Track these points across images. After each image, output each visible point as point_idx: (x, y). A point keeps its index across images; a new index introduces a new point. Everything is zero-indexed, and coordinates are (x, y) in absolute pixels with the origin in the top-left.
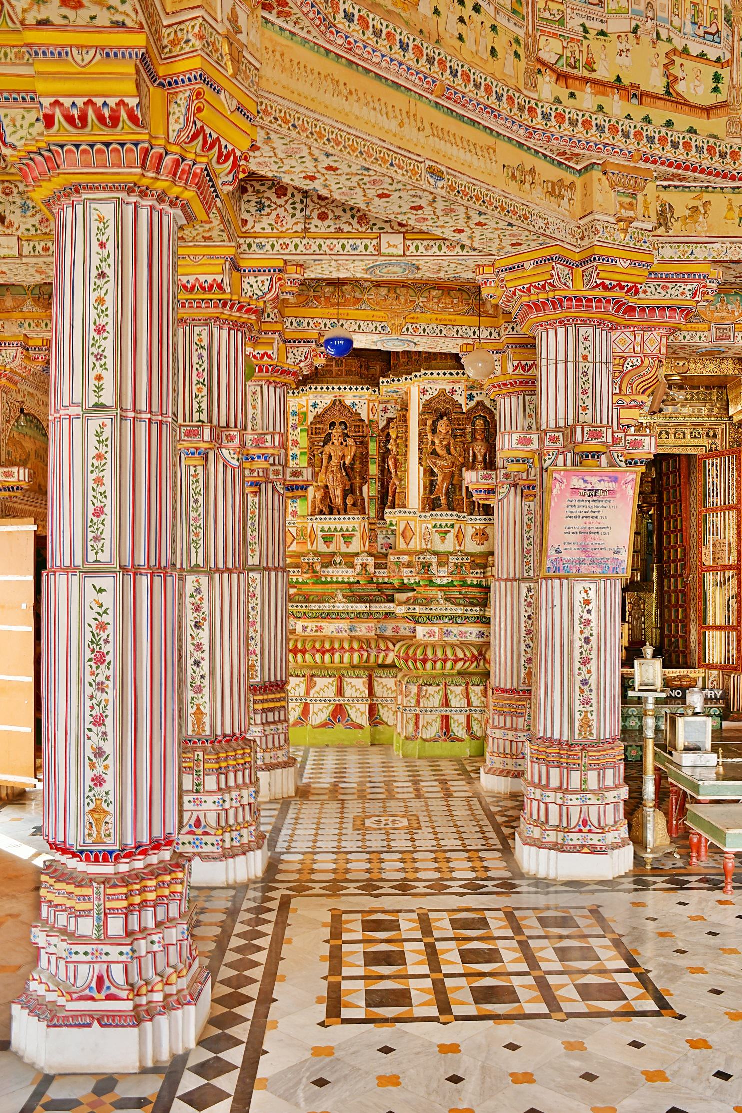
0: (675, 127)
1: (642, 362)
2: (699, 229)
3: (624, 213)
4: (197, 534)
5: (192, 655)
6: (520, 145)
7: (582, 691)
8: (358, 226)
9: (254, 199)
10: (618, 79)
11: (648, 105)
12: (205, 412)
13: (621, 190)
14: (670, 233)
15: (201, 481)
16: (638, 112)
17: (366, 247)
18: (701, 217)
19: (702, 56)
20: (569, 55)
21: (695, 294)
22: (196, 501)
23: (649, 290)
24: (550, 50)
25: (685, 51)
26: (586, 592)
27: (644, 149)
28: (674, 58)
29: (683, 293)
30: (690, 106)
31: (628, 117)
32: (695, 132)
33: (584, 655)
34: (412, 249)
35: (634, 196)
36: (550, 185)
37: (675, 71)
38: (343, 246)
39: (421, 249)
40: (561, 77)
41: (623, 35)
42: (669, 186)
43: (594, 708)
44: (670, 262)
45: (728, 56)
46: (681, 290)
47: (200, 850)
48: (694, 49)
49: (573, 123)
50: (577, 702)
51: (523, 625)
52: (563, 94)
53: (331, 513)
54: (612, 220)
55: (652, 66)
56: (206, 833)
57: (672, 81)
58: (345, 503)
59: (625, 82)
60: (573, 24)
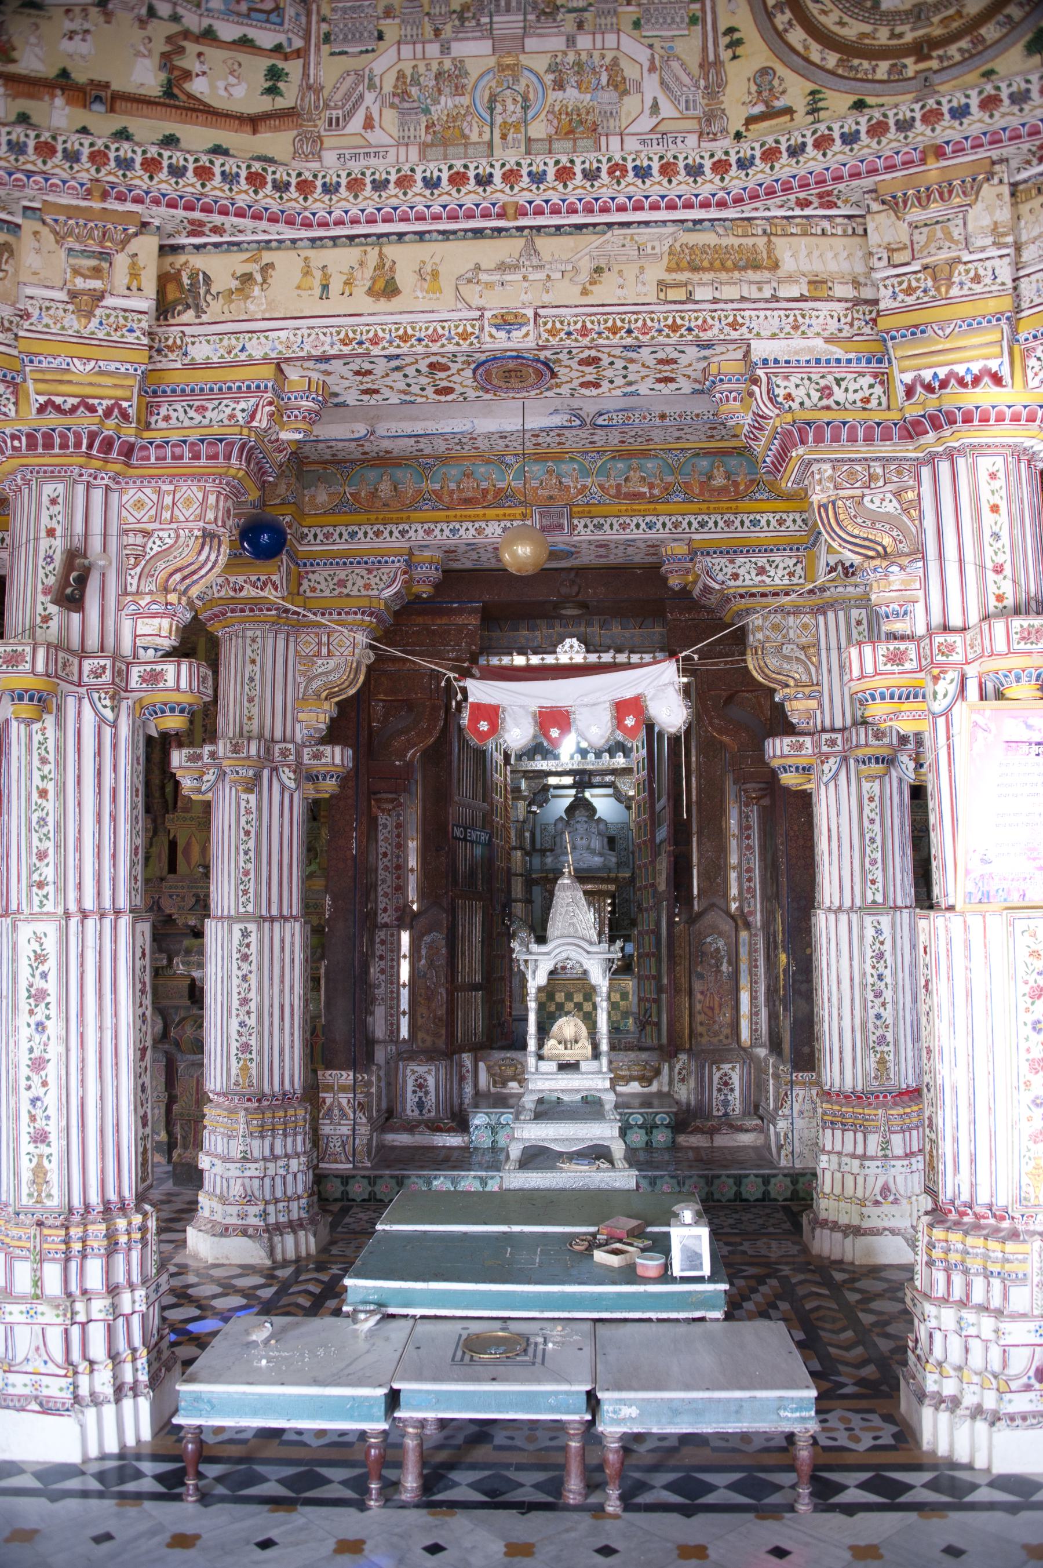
0: (183, 145)
1: (178, 536)
2: (252, 308)
3: (80, 283)
7: (33, 1118)
11: (125, 112)
13: (77, 246)
14: (205, 318)
16: (103, 123)
18: (257, 291)
19: (244, 43)
21: (253, 417)
23: (174, 415)
25: (208, 36)
26: (38, 939)
27: (111, 178)
28: (185, 43)
29: (232, 417)
30: (208, 112)
31: (84, 131)
32: (225, 153)
33: (36, 1054)
35: (105, 256)
42: (205, 245)
43: (54, 1149)
44: (207, 366)
45: (298, 43)
46: (228, 411)
50: (25, 1138)
51: (235, 990)
54: (63, 296)
55: (138, 54)
57: (175, 80)
59: (80, 77)
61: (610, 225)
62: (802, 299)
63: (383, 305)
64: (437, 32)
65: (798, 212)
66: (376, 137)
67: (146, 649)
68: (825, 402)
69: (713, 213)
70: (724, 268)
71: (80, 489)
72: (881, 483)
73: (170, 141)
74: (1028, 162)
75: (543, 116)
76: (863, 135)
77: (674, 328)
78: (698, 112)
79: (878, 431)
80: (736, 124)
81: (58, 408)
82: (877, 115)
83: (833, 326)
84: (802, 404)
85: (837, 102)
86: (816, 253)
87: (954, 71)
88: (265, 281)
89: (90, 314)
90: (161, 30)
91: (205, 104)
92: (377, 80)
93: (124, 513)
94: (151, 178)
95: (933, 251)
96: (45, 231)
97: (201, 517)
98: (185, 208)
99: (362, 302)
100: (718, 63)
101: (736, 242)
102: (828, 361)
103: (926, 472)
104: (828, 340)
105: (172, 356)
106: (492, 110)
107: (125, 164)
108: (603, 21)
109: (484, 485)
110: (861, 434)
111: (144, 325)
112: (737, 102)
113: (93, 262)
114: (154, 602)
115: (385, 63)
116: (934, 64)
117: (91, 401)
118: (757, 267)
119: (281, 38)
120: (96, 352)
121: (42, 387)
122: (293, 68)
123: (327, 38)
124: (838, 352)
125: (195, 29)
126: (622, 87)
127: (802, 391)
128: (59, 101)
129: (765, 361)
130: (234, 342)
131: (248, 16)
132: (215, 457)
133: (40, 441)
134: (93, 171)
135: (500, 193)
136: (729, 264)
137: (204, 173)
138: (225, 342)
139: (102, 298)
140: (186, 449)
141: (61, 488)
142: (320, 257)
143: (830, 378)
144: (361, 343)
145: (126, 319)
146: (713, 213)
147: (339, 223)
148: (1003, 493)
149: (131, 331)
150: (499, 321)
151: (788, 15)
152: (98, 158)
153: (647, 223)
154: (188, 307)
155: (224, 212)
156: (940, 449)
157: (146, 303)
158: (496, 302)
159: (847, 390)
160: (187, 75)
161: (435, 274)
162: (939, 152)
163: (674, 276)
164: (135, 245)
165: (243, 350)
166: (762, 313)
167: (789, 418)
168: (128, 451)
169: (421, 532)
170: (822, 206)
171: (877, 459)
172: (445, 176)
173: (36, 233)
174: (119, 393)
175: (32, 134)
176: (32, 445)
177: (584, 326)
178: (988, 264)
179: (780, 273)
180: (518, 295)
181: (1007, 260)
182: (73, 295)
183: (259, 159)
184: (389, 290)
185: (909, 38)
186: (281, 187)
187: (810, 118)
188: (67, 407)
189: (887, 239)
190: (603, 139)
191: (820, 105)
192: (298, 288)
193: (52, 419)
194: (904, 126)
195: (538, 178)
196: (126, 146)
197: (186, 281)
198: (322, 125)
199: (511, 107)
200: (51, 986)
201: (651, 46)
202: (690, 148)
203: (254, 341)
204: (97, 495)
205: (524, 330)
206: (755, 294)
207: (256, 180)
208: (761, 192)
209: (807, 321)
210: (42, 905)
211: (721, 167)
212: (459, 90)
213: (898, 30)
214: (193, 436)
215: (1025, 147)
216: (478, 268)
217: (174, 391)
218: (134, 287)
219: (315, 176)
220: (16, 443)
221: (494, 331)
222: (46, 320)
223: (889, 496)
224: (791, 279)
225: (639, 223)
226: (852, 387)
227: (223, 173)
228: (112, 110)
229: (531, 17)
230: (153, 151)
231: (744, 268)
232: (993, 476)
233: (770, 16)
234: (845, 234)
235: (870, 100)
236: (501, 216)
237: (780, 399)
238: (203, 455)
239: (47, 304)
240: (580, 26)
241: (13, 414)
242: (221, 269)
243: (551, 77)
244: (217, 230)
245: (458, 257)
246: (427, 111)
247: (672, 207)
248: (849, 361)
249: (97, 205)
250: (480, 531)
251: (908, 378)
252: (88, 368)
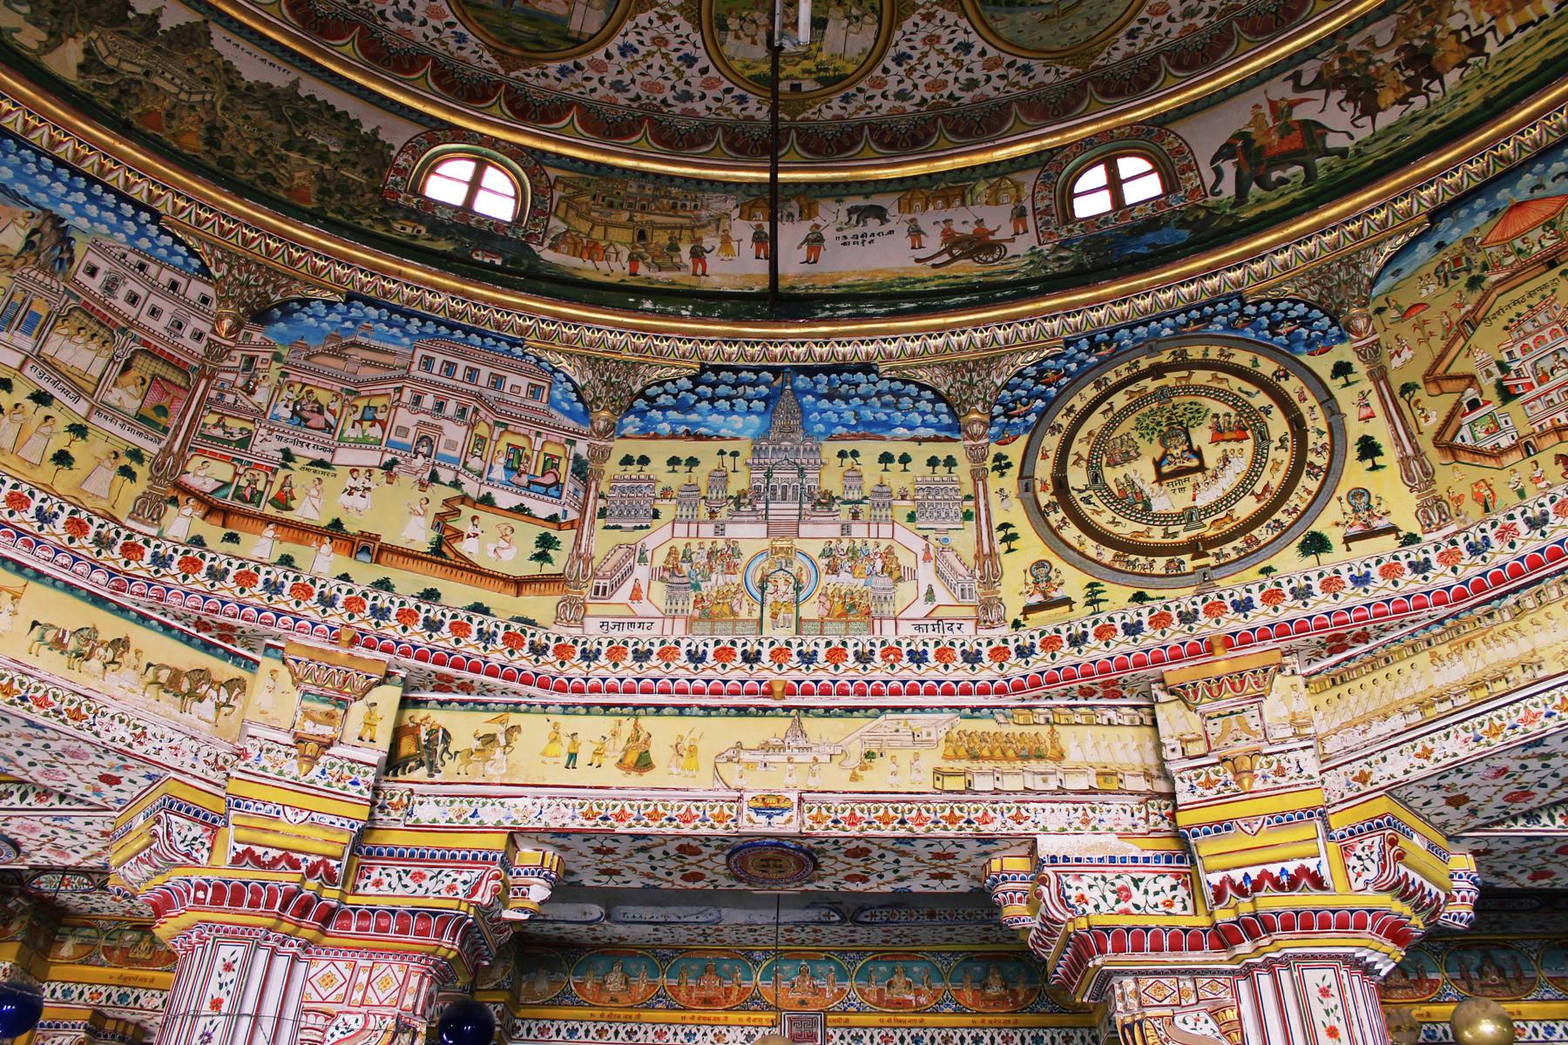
0: (443, 600)
2: (490, 770)
3: (309, 728)
6: (97, 600)
10: (337, 524)
11: (390, 565)
13: (314, 690)
14: (438, 777)
16: (365, 573)
18: (499, 751)
19: (520, 510)
20: (243, 483)
21: (474, 891)
23: (386, 880)
24: (205, 474)
25: (487, 501)
27: (364, 625)
28: (461, 507)
29: (451, 888)
31: (345, 577)
32: (486, 611)
35: (342, 703)
36: (164, 675)
37: (462, 524)
40: (212, 509)
41: (363, 470)
42: (449, 702)
44: (432, 828)
45: (573, 515)
46: (448, 881)
48: (505, 499)
49: (216, 575)
52: (213, 532)
55: (414, 512)
59: (351, 527)
60: (268, 447)
61: (883, 709)
62: (1091, 791)
63: (634, 779)
64: (713, 514)
65: (1081, 701)
66: (642, 608)
68: (1122, 906)
69: (992, 700)
70: (1005, 757)
71: (263, 955)
72: (1193, 1001)
73: (431, 595)
74: (1319, 654)
75: (815, 598)
76: (1146, 626)
77: (952, 819)
78: (975, 601)
79: (1186, 940)
80: (1014, 613)
81: (257, 861)
82: (1158, 606)
83: (1127, 821)
84: (1097, 907)
85: (1117, 596)
86: (1103, 744)
87: (1232, 568)
88: (508, 744)
89: (314, 760)
90: (440, 493)
91: (472, 563)
92: (648, 555)
93: (309, 989)
94: (405, 629)
95: (1231, 743)
96: (284, 670)
97: (399, 1000)
98: (435, 662)
99: (611, 775)
100: (993, 554)
101: (1018, 730)
102: (1123, 859)
103: (1243, 986)
104: (1121, 836)
105: (394, 815)
106: (763, 589)
107: (380, 613)
108: (878, 513)
110: (1166, 943)
111: (371, 779)
112: (1014, 591)
113: (328, 708)
115: (659, 540)
116: (1212, 561)
117: (295, 856)
118: (1040, 757)
119: (558, 510)
120: (313, 803)
121: (243, 834)
122: (566, 538)
123: (602, 513)
124: (1133, 849)
125: (474, 496)
126: (896, 575)
127: (1096, 893)
128: (326, 548)
129: (1054, 859)
131: (528, 488)
132: (425, 933)
133: (228, 896)
134: (346, 617)
135: (767, 671)
136: (1010, 753)
137: (460, 629)
138: (456, 805)
139: (329, 745)
140: (393, 921)
141: (240, 951)
142: (568, 723)
143: (1127, 878)
144: (605, 819)
145: (351, 770)
146: (992, 700)
147: (595, 690)
148: (1339, 1013)
149: (355, 783)
150: (760, 804)
151: (1061, 514)
152: (353, 604)
153: (922, 709)
154: (422, 764)
155: (475, 669)
156: (1259, 960)
157: (375, 754)
158: (756, 783)
159: (1146, 892)
160: (459, 535)
161: (693, 750)
162: (1227, 643)
163: (952, 764)
164: (376, 694)
166: (1048, 806)
167: (1083, 923)
168: (327, 915)
170: (1106, 695)
171: (1186, 972)
172: (711, 650)
173: (273, 672)
174: (329, 849)
175: (291, 576)
176: (218, 898)
177: (853, 814)
178: (1290, 755)
179: (1065, 763)
180: (782, 778)
181: (1311, 752)
182: (300, 740)
183: (519, 620)
184: (644, 763)
185: (1183, 537)
186: (538, 650)
187: (1090, 609)
188: (267, 859)
189: (1178, 731)
190: (877, 623)
191: (1099, 596)
192: (544, 754)
193: (249, 874)
194: (1187, 618)
195: (808, 658)
196: (385, 595)
197: (424, 736)
198: (587, 592)
199: (782, 588)
201: (925, 537)
202: (967, 635)
203: (488, 806)
204: (281, 964)
205: (787, 815)
206: (1040, 786)
207: (513, 641)
208: (1043, 680)
209: (1098, 815)
211: (1000, 654)
212: (731, 569)
213: (1171, 530)
214: (405, 905)
215: (1314, 638)
216: (739, 746)
218: (366, 739)
219: (575, 642)
220: (200, 894)
221: (753, 815)
222: (264, 762)
223: (1204, 1015)
224: (1077, 770)
225: (914, 708)
226: (1152, 888)
227: (480, 631)
228: (377, 561)
229: (807, 506)
230: (411, 603)
231: (1027, 758)
232: (1325, 992)
233: (1044, 515)
234: (1132, 725)
235: (1150, 593)
236: (769, 693)
237: (1072, 901)
239: (269, 745)
240: (855, 516)
241: (204, 861)
243: (826, 561)
244: (466, 687)
245: (721, 732)
246: (696, 587)
247: (948, 692)
248: (1147, 860)
249: (343, 652)
251: (1215, 879)
252: (300, 818)
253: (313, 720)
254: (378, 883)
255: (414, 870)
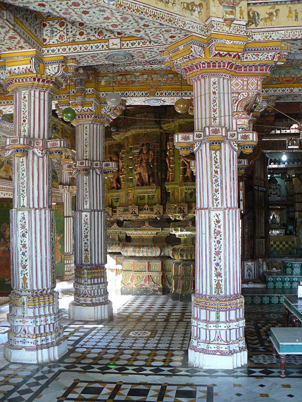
1: (248, 95)
3: (228, 17)
4: (23, 191)
5: (21, 250)
7: (216, 269)
8: (98, 37)
9: (50, 29)
12: (27, 131)
13: (226, 5)
14: (258, 27)
15: (25, 165)
17: (103, 46)
18: (274, 18)
22: (23, 174)
26: (217, 216)
29: (267, 58)
33: (217, 250)
34: (125, 45)
36: (185, 5)
38: (92, 47)
39: (130, 45)
42: (256, 3)
43: (223, 278)
44: (259, 42)
46: (266, 56)
47: (26, 345)
50: (213, 275)
53: (142, 185)
54: (222, 20)
56: (29, 337)
58: (149, 181)
67: (239, 128)
71: (221, 79)
81: (221, 55)
88: (277, 15)
93: (232, 87)
109: (293, 76)
113: (231, 10)
114: (244, 114)
117: (230, 53)
130: (267, 34)
132: (263, 70)
138: (265, 34)
140: (253, 67)
141: (216, 79)
145: (240, 27)
149: (242, 31)
154: (253, 23)
165: (271, 37)
169: (272, 91)
174: (239, 50)
182: (226, 20)
192: (288, 17)
193: (218, 58)
200: (222, 230)
203: (274, 34)
210: (217, 206)
214: (257, 64)
217: (249, 49)
218: (242, 17)
220: (204, 65)
238: (259, 69)
239: (218, 23)
241: (203, 56)
242: (263, 11)
250: (292, 91)
253: (228, 14)
254: (246, 58)
255: (256, 53)
